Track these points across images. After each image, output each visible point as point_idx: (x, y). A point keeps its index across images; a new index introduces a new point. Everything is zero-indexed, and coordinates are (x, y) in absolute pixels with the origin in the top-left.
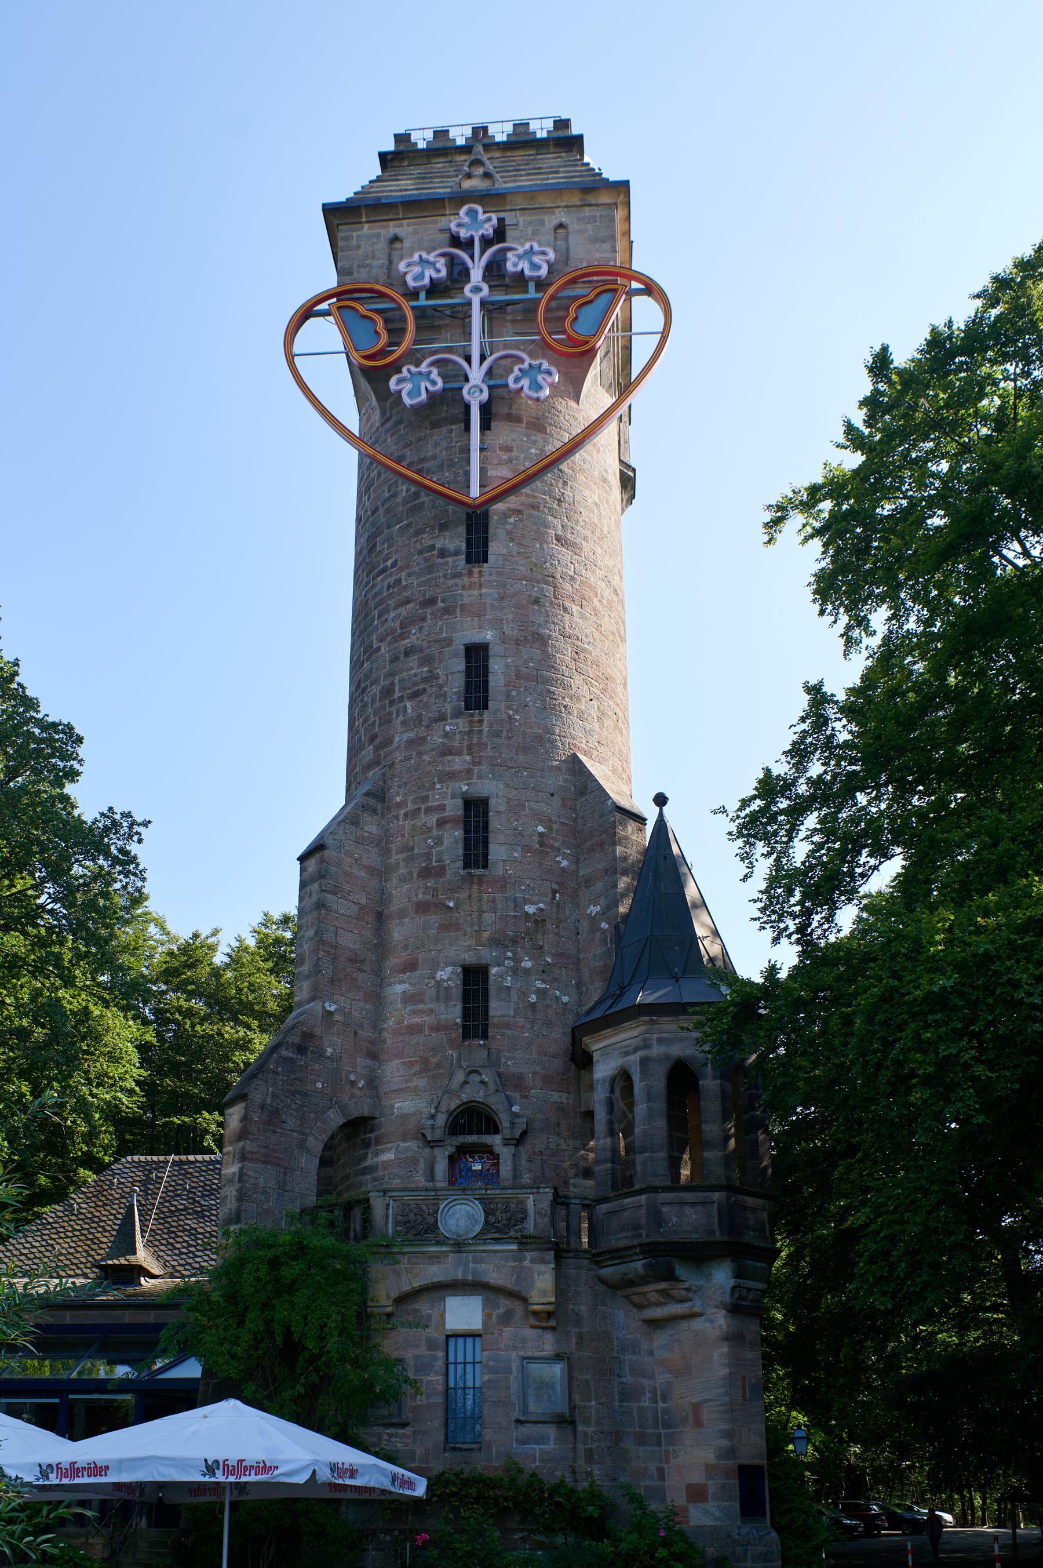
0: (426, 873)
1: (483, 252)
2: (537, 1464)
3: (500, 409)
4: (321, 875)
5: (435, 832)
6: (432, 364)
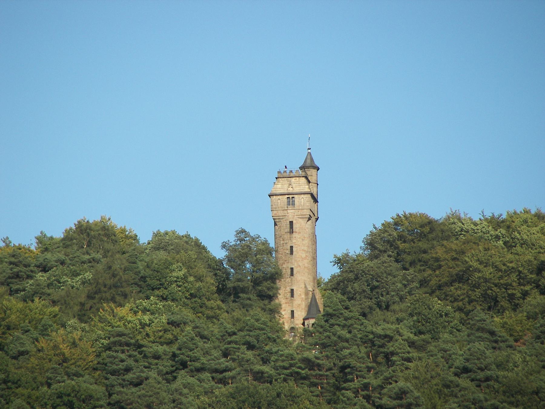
0: (286, 299)
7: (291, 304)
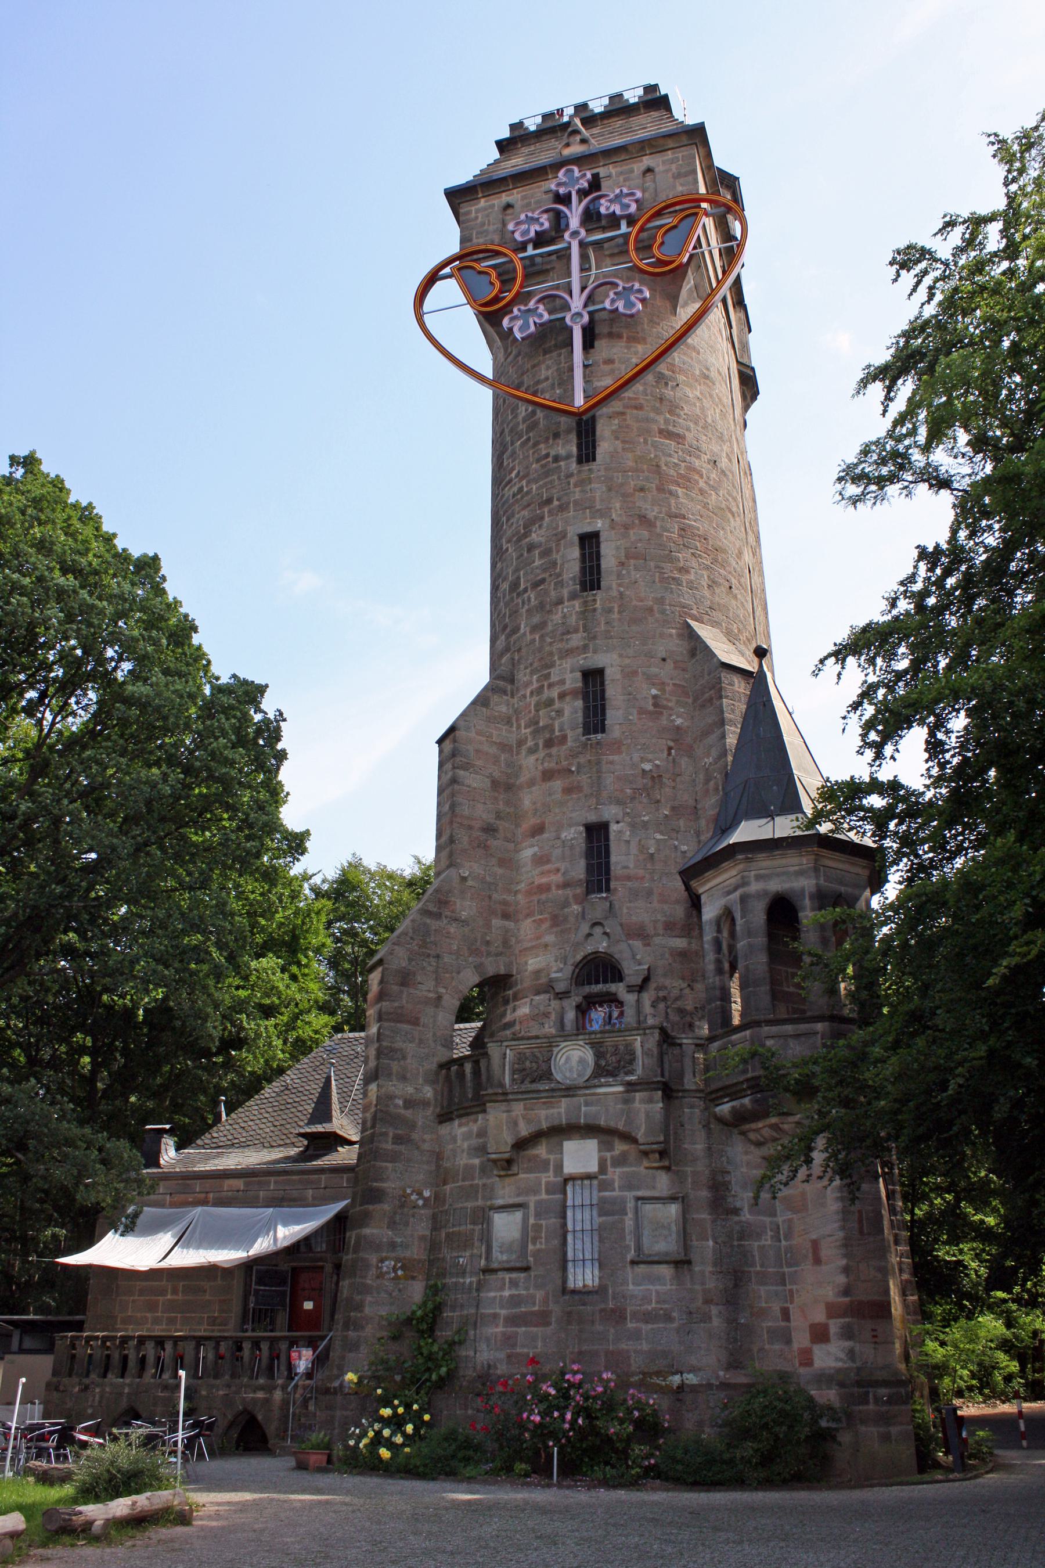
0: (549, 744)
1: (580, 201)
3: (601, 329)
4: (454, 754)
5: (557, 705)
6: (539, 301)
7: (584, 779)
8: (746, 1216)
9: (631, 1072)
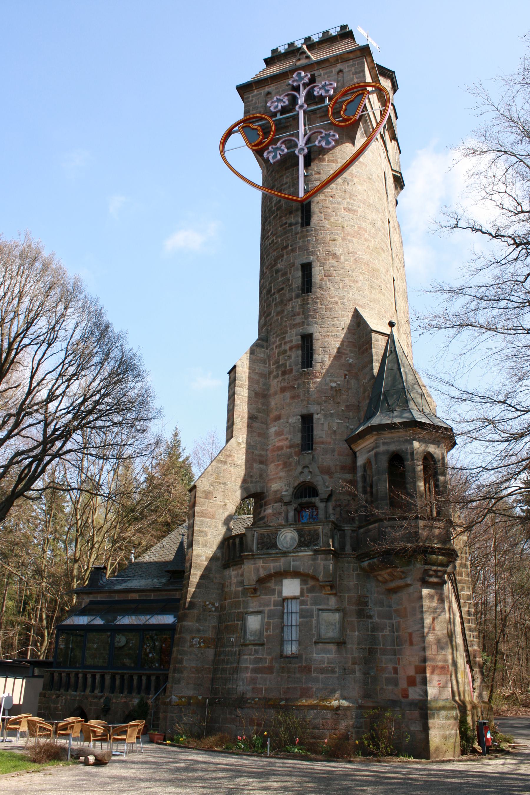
0: (284, 373)
2: (326, 665)
5: (288, 353)
6: (282, 143)
8: (376, 619)
9: (316, 545)
